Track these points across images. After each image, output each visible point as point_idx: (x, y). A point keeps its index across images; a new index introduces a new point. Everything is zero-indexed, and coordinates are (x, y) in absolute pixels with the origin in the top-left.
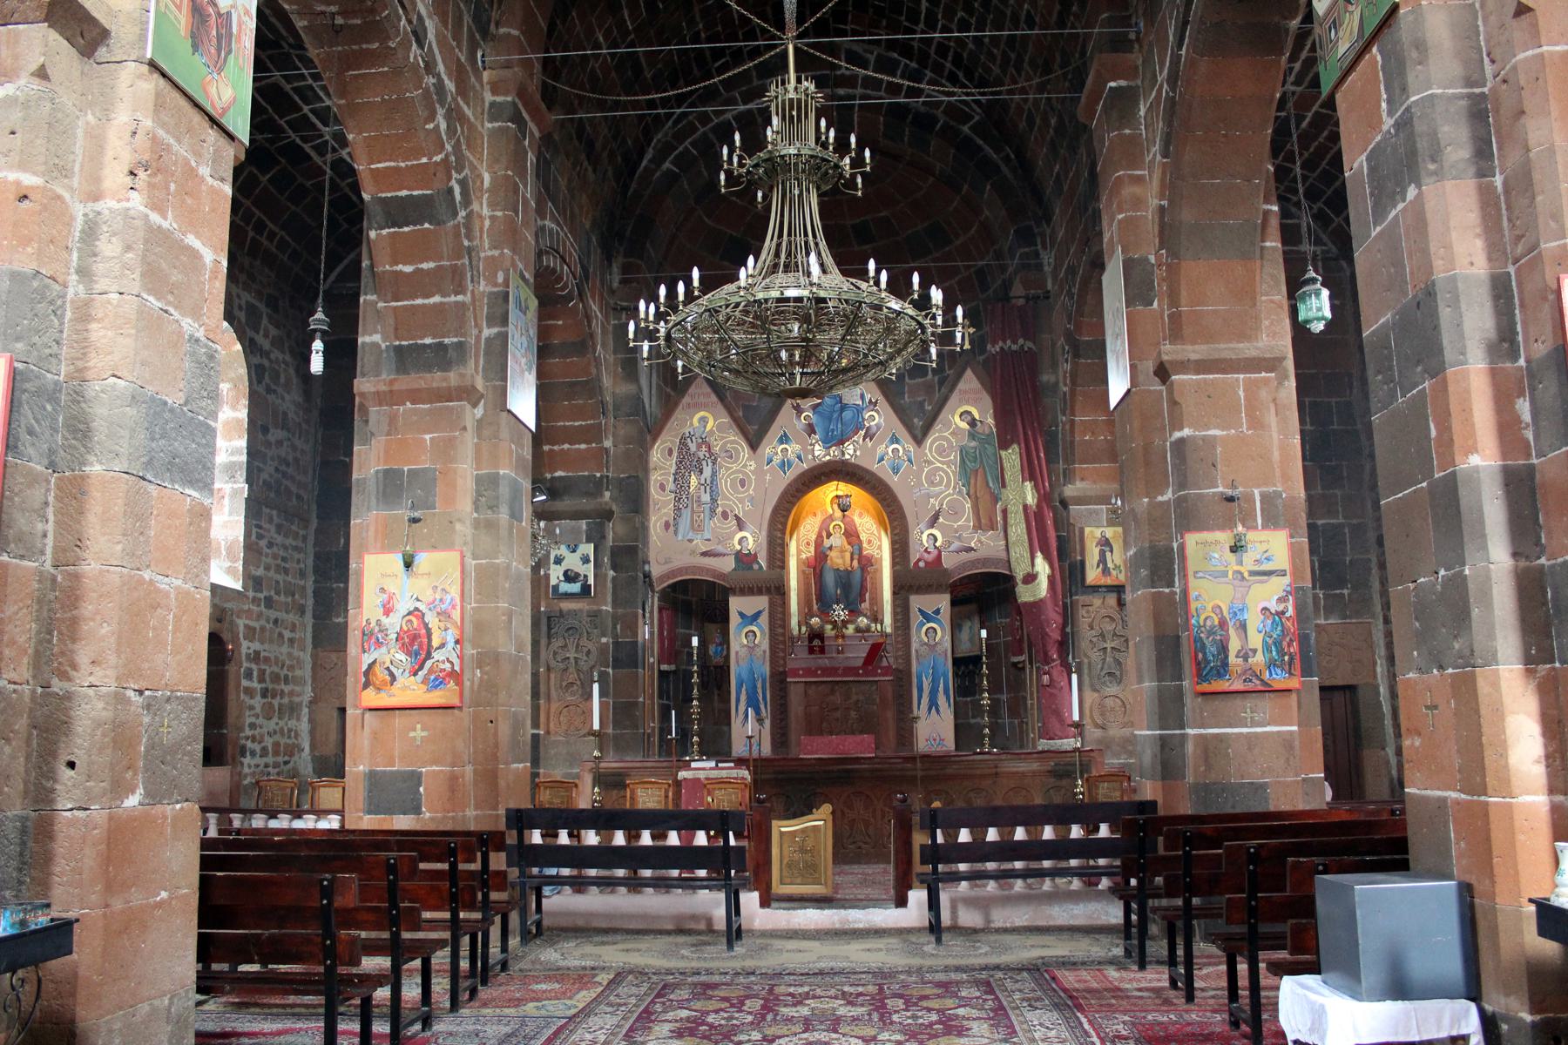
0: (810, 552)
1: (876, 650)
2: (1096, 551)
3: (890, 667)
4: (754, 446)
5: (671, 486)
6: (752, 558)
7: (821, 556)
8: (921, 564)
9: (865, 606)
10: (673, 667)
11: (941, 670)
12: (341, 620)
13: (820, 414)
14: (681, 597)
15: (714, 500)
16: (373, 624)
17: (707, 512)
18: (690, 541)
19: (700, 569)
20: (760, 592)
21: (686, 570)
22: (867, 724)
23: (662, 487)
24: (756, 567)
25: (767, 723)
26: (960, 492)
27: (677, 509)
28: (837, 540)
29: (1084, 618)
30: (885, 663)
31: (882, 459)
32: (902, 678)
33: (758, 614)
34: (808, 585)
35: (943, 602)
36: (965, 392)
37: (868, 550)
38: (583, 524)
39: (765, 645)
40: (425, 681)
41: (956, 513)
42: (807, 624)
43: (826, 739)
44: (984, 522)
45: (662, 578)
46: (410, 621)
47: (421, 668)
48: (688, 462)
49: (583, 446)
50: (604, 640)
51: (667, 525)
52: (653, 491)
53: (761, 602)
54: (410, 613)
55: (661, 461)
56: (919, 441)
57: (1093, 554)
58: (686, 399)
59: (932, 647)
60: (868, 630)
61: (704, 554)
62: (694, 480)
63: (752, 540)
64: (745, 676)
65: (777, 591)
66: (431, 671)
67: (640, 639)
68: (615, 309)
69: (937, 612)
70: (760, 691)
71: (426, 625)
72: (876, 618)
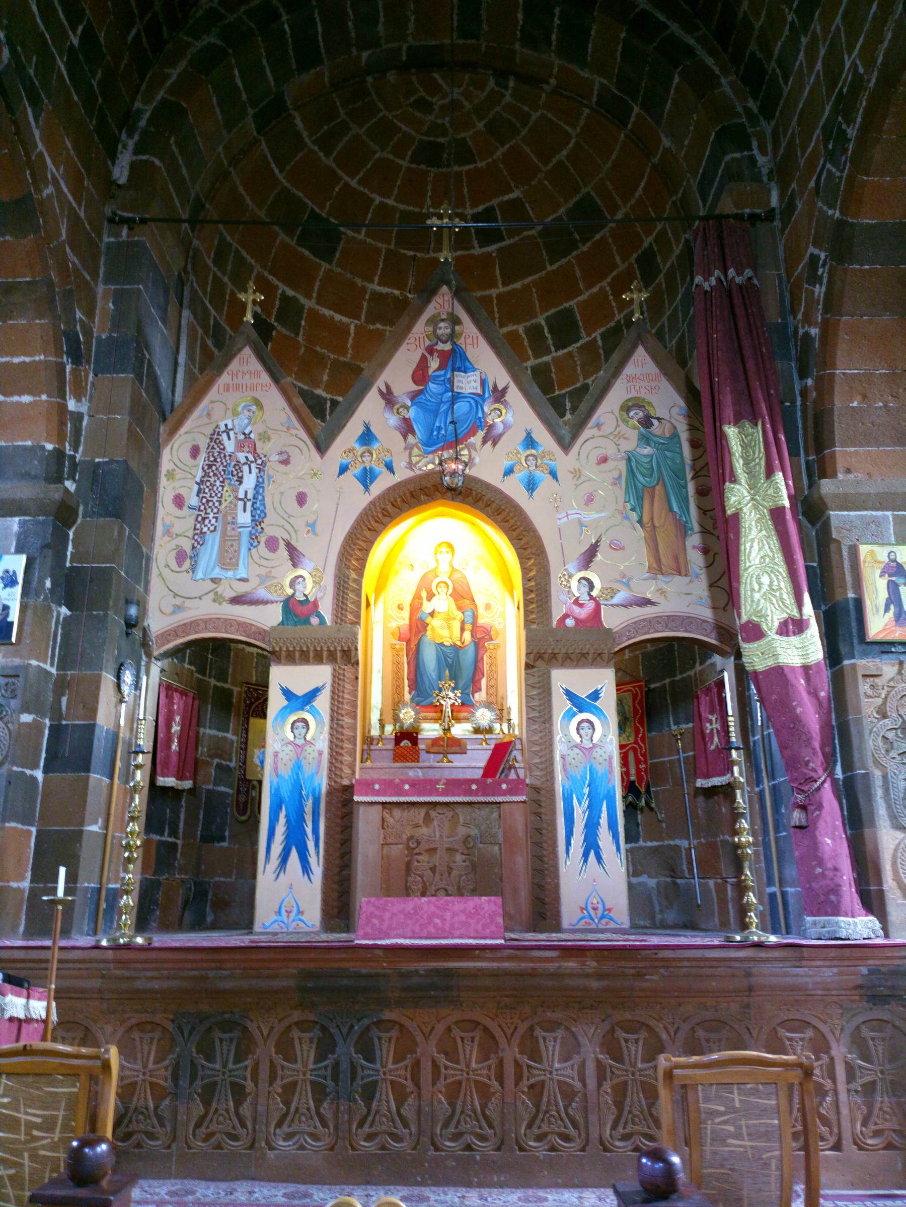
0: (403, 619)
1: (501, 750)
2: (882, 584)
3: (520, 782)
4: (322, 447)
5: (194, 501)
6: (311, 607)
7: (418, 626)
8: (570, 622)
9: (480, 696)
10: (188, 784)
11: (602, 791)
13: (422, 406)
14: (213, 682)
15: (258, 520)
17: (245, 539)
18: (213, 580)
19: (228, 623)
20: (318, 659)
21: (206, 623)
22: (481, 877)
23: (179, 501)
24: (314, 621)
25: (318, 870)
26: (627, 518)
27: (199, 536)
28: (443, 603)
29: (866, 701)
30: (512, 776)
31: (509, 472)
32: (540, 799)
33: (314, 693)
34: (398, 665)
35: (603, 681)
36: (636, 378)
37: (484, 619)
38: (14, 524)
39: (323, 744)
41: (617, 547)
42: (396, 719)
43: (410, 904)
44: (667, 564)
45: (166, 636)
48: (219, 468)
49: (26, 399)
50: (26, 718)
51: (181, 556)
52: (165, 510)
53: (318, 676)
55: (178, 468)
56: (566, 447)
57: (876, 590)
58: (225, 379)
59: (588, 752)
60: (490, 730)
61: (237, 600)
62: (227, 495)
63: (313, 582)
64: (285, 793)
65: (344, 656)
67: (103, 719)
68: (111, 221)
69: (595, 695)
70: (309, 818)
72: (502, 714)
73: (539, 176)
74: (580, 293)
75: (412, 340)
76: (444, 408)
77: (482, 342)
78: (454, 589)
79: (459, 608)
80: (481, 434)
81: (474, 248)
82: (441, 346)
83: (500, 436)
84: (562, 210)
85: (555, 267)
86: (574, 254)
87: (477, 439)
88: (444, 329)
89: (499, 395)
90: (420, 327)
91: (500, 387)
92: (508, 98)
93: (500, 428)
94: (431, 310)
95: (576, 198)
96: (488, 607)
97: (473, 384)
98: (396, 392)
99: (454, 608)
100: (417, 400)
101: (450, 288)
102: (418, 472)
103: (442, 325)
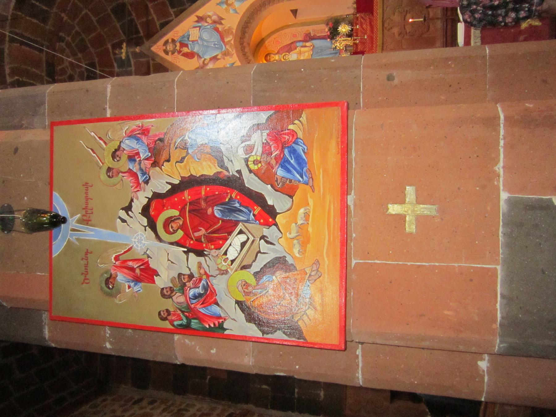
12: (322, 394)
16: (169, 305)
40: (289, 191)
46: (168, 222)
47: (259, 199)
54: (152, 225)
66: (266, 177)
71: (175, 189)
73: (102, 33)
74: (153, 19)
75: (175, 61)
76: (205, 43)
77: (176, 29)
78: (287, 52)
79: (296, 49)
80: (218, 26)
81: (131, 70)
82: (178, 48)
83: (218, 16)
84: (118, 25)
85: (141, 32)
86: (136, 21)
87: (220, 27)
88: (170, 47)
89: (200, 19)
90: (169, 58)
91: (196, 19)
92: (69, 39)
93: (215, 18)
94: (163, 54)
95: (112, 16)
96: (295, 36)
97: (195, 32)
98: (197, 66)
99: (295, 51)
100: (201, 56)
101: (152, 46)
102: (234, 51)
103: (168, 48)
